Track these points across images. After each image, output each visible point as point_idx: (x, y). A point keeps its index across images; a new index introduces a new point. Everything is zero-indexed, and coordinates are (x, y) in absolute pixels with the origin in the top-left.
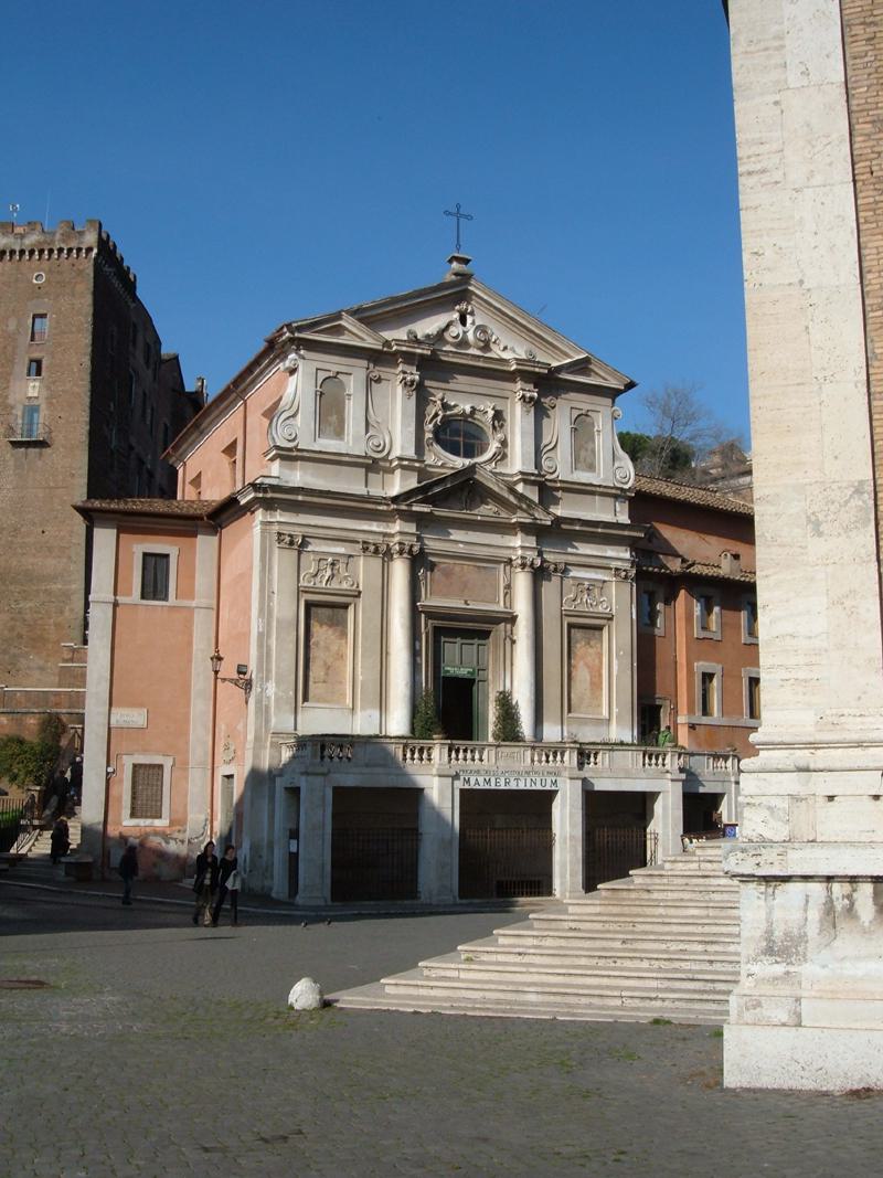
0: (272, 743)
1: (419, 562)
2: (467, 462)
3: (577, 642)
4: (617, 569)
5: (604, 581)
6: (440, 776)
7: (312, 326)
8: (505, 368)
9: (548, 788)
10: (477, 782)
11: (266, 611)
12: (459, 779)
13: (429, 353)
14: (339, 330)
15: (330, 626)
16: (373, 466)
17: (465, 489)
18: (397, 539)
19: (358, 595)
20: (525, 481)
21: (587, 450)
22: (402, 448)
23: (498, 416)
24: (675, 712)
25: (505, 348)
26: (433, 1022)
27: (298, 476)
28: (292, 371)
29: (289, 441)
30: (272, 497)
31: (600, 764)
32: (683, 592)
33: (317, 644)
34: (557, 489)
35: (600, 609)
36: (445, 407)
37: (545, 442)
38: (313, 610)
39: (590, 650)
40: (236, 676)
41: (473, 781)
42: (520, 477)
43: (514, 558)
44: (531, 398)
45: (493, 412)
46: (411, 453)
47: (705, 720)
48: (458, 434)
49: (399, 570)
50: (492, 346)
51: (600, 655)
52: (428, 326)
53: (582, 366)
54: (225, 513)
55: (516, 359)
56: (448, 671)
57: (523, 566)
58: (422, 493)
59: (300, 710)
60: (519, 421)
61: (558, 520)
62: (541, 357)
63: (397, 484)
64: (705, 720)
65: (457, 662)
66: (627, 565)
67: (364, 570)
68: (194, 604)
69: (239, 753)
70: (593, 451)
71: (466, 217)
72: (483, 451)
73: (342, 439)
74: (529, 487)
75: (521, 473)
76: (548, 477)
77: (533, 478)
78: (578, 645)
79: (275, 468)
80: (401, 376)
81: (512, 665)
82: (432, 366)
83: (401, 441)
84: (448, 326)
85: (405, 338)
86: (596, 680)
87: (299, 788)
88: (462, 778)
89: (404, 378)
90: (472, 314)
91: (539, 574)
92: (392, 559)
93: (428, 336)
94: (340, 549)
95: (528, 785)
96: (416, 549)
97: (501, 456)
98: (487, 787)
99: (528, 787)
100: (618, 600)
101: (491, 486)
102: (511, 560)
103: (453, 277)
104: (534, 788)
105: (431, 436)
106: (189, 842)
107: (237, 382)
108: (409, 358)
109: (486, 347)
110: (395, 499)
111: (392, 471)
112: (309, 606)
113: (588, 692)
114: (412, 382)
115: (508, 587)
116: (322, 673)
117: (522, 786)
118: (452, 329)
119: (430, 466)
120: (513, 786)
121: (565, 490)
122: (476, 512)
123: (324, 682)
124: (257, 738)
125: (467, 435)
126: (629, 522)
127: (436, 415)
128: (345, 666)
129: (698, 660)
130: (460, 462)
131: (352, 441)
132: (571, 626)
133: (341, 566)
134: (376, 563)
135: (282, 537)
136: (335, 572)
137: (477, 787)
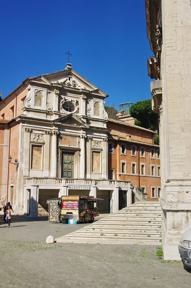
0: (23, 178)
1: (59, 136)
2: (70, 113)
3: (94, 155)
4: (104, 139)
5: (101, 141)
6: (64, 186)
7: (34, 79)
8: (80, 91)
9: (88, 189)
11: (22, 147)
12: (68, 187)
13: (62, 87)
14: (41, 80)
15: (38, 151)
16: (48, 113)
17: (69, 119)
18: (54, 130)
19: (44, 144)
20: (83, 118)
21: (97, 111)
22: (55, 109)
23: (77, 102)
24: (116, 171)
25: (79, 86)
26: (72, 245)
27: (30, 115)
28: (29, 90)
29: (28, 106)
30: (24, 120)
31: (100, 184)
32: (118, 145)
33: (34, 155)
34: (90, 120)
35: (100, 148)
36: (65, 100)
37: (88, 109)
38: (34, 147)
39: (97, 157)
40: (15, 162)
41: (71, 188)
42: (82, 117)
43: (80, 135)
44: (85, 98)
45: (76, 101)
46: (57, 110)
47: (123, 174)
48: (68, 106)
49: (54, 138)
50: (76, 86)
51: (99, 158)
52: (61, 81)
53: (97, 91)
54: (12, 124)
55: (82, 89)
56: (65, 162)
57: (82, 137)
58: (60, 120)
59: (30, 170)
60: (82, 103)
61: (91, 127)
62: (88, 89)
63: (54, 117)
64: (123, 174)
65: (67, 160)
66: (106, 138)
67: (45, 138)
68: (3, 145)
69: (15, 181)
70: (99, 111)
71: (70, 54)
72: (73, 110)
73: (41, 106)
74: (84, 119)
75: (83, 116)
76: (89, 117)
77: (85, 117)
78: (95, 156)
79: (25, 113)
80: (55, 92)
81: (80, 160)
82: (62, 91)
83: (55, 108)
84: (66, 80)
85: (56, 83)
86: (99, 164)
87: (30, 189)
88: (69, 187)
89: (56, 92)
90: (72, 78)
91: (86, 140)
92: (52, 135)
93: (61, 83)
95: (84, 188)
96: (58, 133)
97: (77, 112)
98: (75, 189)
99: (84, 189)
100: (104, 146)
101: (75, 118)
102: (80, 136)
103: (67, 69)
104: (85, 189)
105: (62, 106)
106: (2, 202)
107: (14, 92)
108: (57, 88)
109: (75, 86)
110: (54, 121)
111: (52, 115)
112: (33, 146)
113: (97, 167)
114: (58, 93)
115: (79, 142)
116: (35, 162)
117: (82, 189)
118: (67, 81)
119: (62, 114)
120: (80, 189)
121: (92, 120)
122: (74, 125)
123: (36, 164)
124: (20, 177)
125: (70, 106)
126: (106, 128)
127: (63, 101)
128: (41, 160)
130: (69, 113)
131: (43, 107)
132: (93, 152)
133: (40, 136)
134: (49, 136)
135: (26, 129)
136: (39, 138)
137: (72, 189)
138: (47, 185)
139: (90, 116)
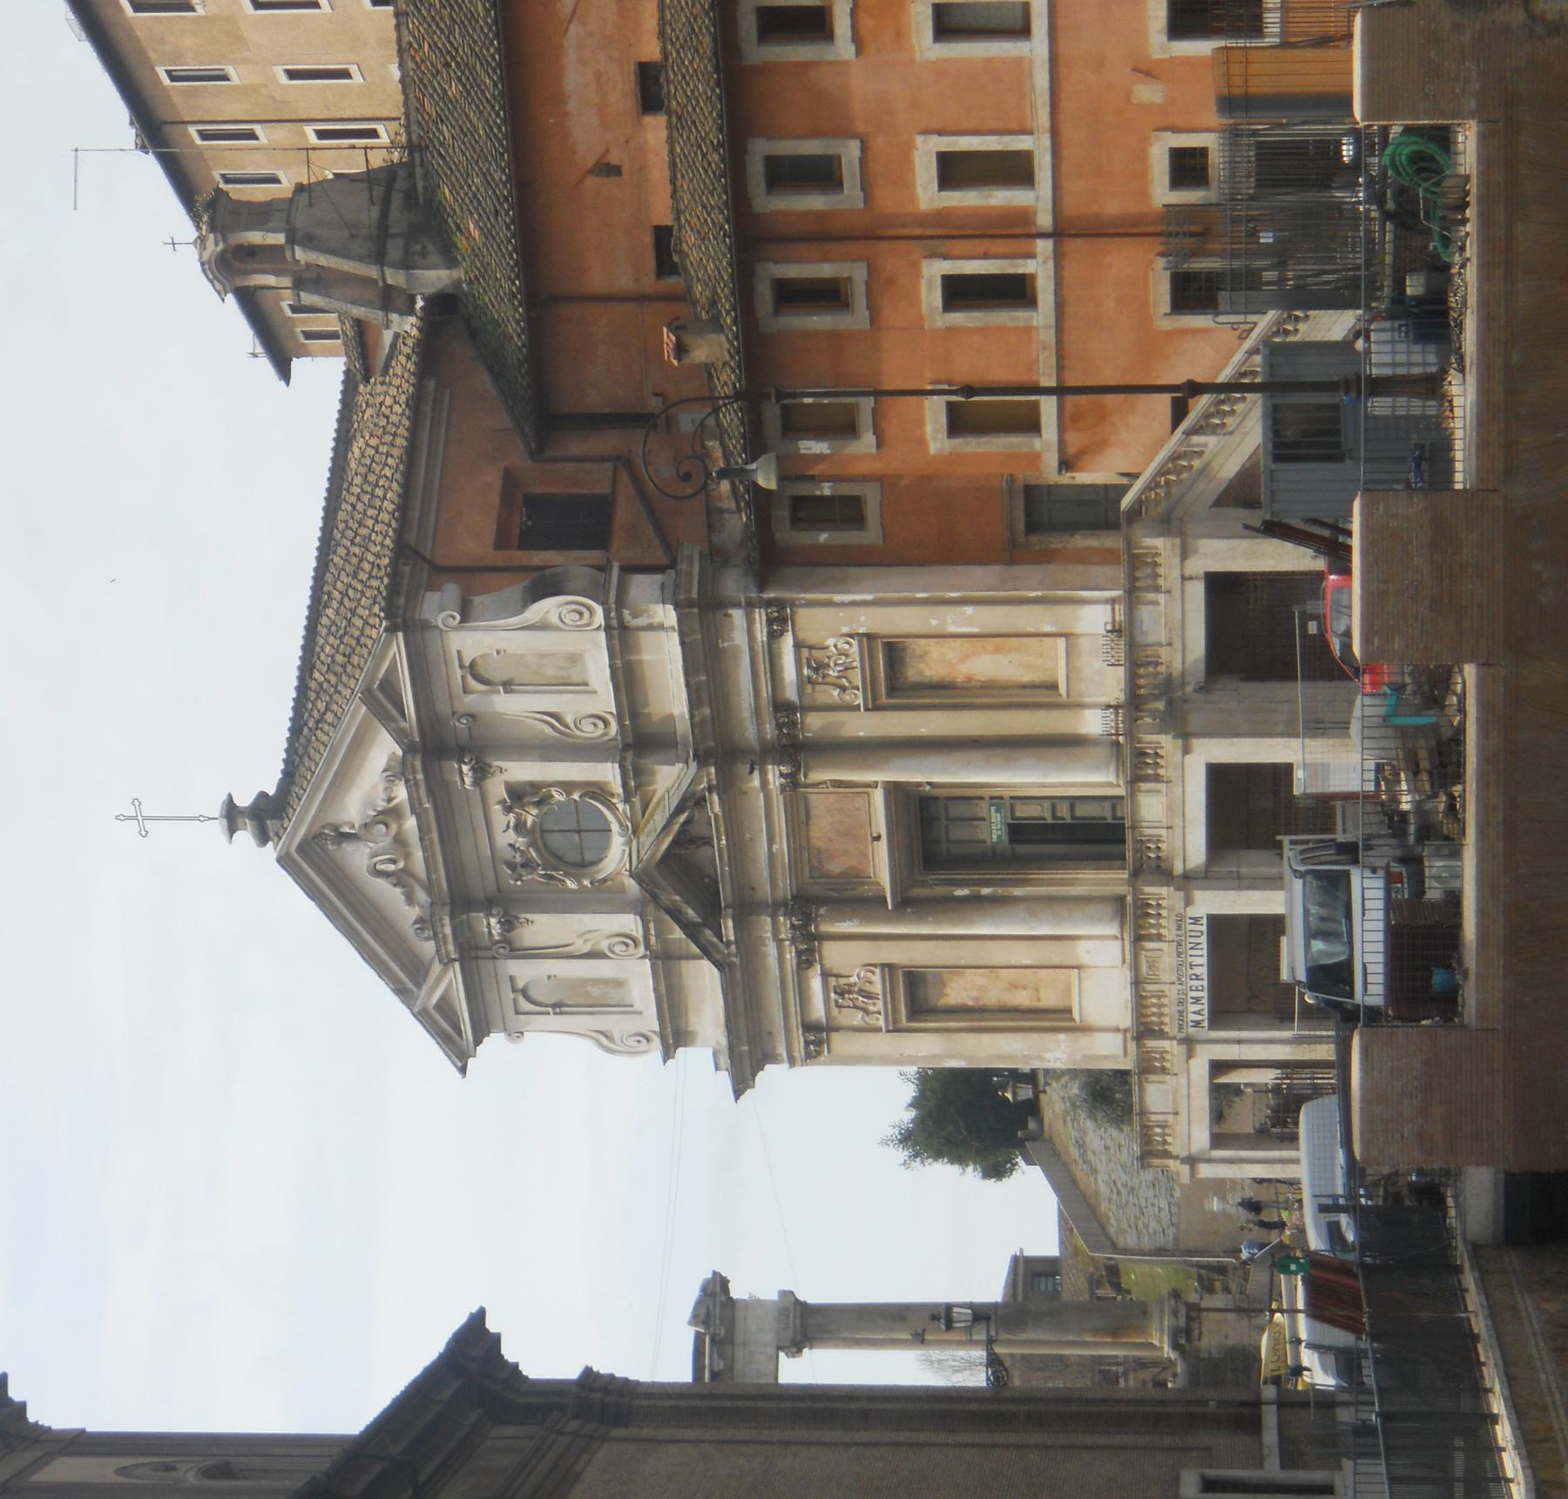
5: (798, 646)
9: (1204, 929)
10: (1198, 1013)
14: (445, 1007)
15: (945, 985)
33: (976, 999)
94: (816, 983)
98: (1205, 1001)
99: (1205, 952)
104: (1205, 946)
117: (1204, 961)
120: (1203, 971)
129: (922, 443)
137: (1206, 1012)
138: (1183, 1109)
139: (608, 716)
